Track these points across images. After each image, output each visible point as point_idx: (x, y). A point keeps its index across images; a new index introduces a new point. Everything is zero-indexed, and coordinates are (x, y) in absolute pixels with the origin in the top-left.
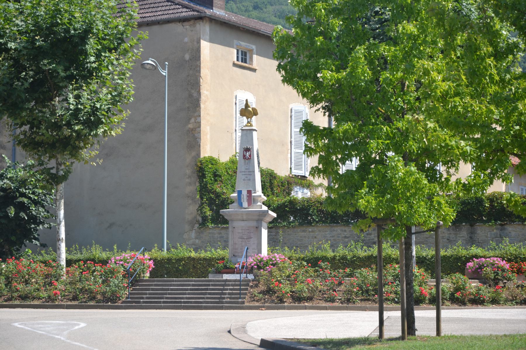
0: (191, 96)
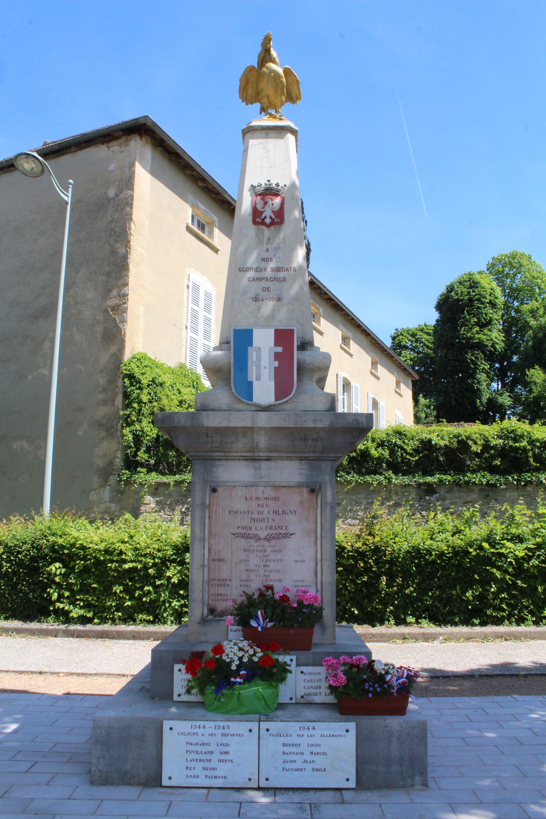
0: (114, 252)
